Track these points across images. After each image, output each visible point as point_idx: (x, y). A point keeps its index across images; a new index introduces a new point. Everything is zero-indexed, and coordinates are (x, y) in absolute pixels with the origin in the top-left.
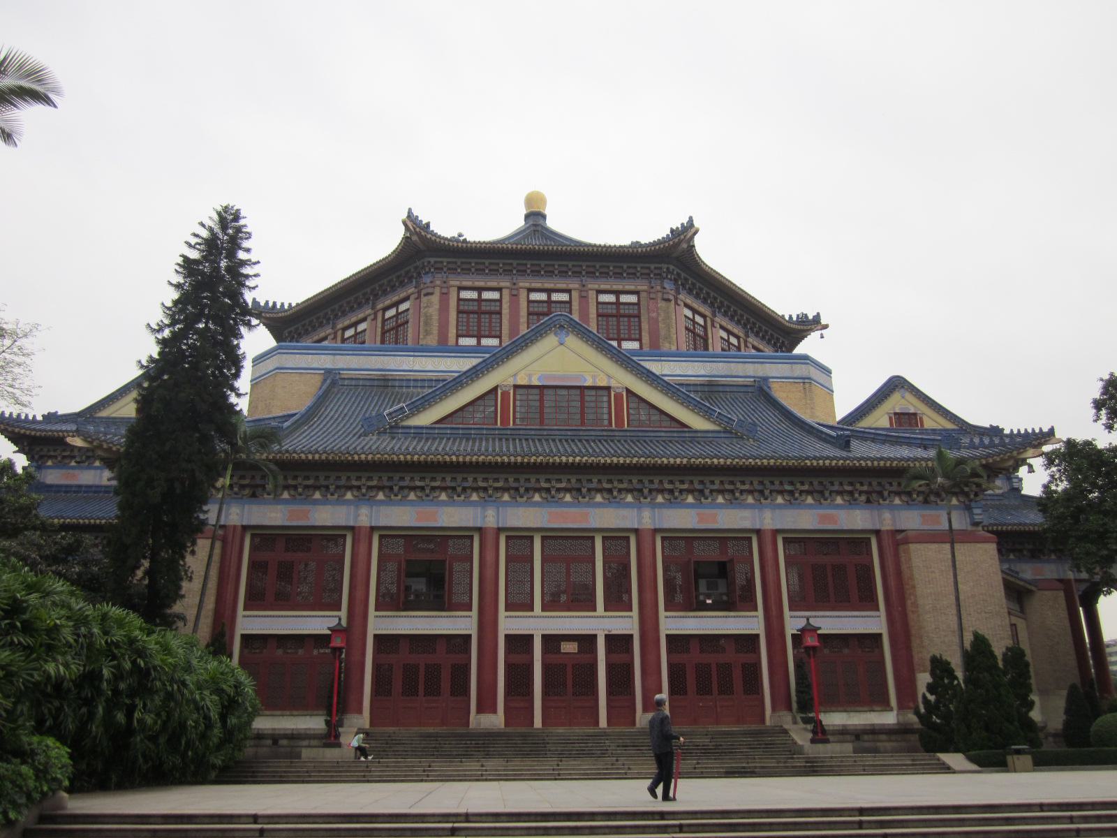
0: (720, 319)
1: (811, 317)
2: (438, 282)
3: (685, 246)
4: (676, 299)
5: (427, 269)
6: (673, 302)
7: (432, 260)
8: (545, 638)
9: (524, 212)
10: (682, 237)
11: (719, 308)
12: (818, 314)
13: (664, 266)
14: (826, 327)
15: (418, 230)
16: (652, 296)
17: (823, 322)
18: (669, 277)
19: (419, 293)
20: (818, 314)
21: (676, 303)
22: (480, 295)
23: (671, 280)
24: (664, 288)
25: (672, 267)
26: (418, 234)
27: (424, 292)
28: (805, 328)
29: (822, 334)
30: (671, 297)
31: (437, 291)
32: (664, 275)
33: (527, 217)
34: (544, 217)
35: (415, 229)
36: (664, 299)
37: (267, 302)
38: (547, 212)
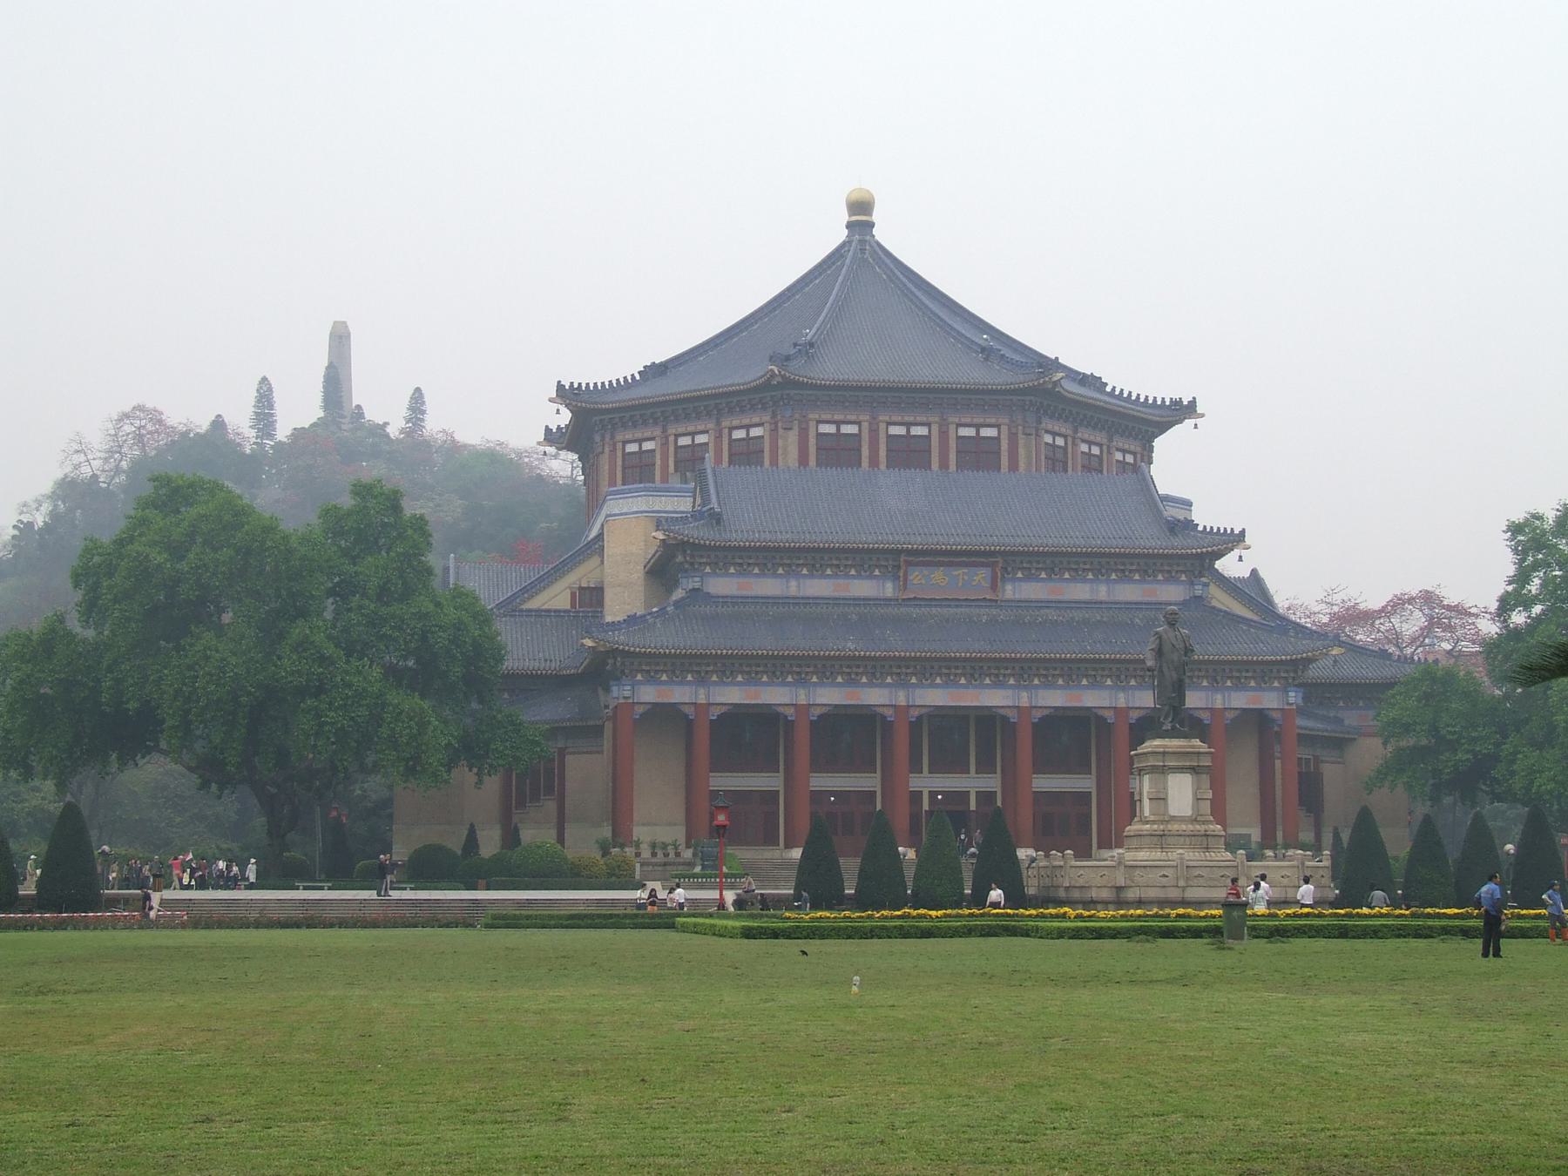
0: (1084, 433)
1: (1185, 403)
2: (797, 416)
3: (1050, 386)
4: (1037, 430)
5: (786, 401)
6: (1033, 437)
7: (792, 392)
8: (933, 794)
9: (844, 217)
10: (1047, 379)
11: (1082, 420)
12: (1194, 398)
13: (1028, 398)
14: (1202, 416)
15: (783, 373)
16: (1014, 430)
17: (1199, 410)
19: (776, 423)
20: (1194, 398)
21: (1037, 435)
22: (838, 429)
24: (1027, 422)
25: (1032, 398)
26: (784, 376)
27: (780, 425)
28: (1174, 419)
29: (1196, 425)
30: (1034, 433)
31: (796, 428)
32: (1027, 407)
33: (849, 226)
34: (871, 225)
35: (780, 372)
36: (1026, 434)
37: (572, 383)
38: (877, 216)
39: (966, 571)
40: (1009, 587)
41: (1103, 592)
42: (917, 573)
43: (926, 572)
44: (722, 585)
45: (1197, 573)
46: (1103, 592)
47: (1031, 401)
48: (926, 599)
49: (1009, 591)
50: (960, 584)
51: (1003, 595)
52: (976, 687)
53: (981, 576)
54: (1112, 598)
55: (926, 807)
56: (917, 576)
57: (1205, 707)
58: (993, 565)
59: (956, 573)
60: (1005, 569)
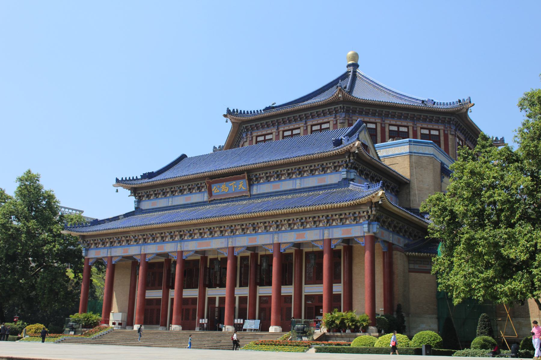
7: (244, 126)
18: (342, 111)
23: (343, 112)
25: (341, 105)
36: (340, 123)
39: (235, 183)
40: (255, 188)
41: (298, 184)
42: (215, 187)
43: (218, 186)
44: (146, 205)
45: (345, 165)
46: (298, 184)
47: (340, 107)
48: (219, 200)
49: (255, 190)
50: (234, 190)
51: (253, 193)
52: (209, 239)
53: (241, 185)
54: (302, 186)
55: (217, 305)
56: (215, 189)
57: (319, 239)
58: (243, 178)
59: (230, 185)
60: (250, 180)
